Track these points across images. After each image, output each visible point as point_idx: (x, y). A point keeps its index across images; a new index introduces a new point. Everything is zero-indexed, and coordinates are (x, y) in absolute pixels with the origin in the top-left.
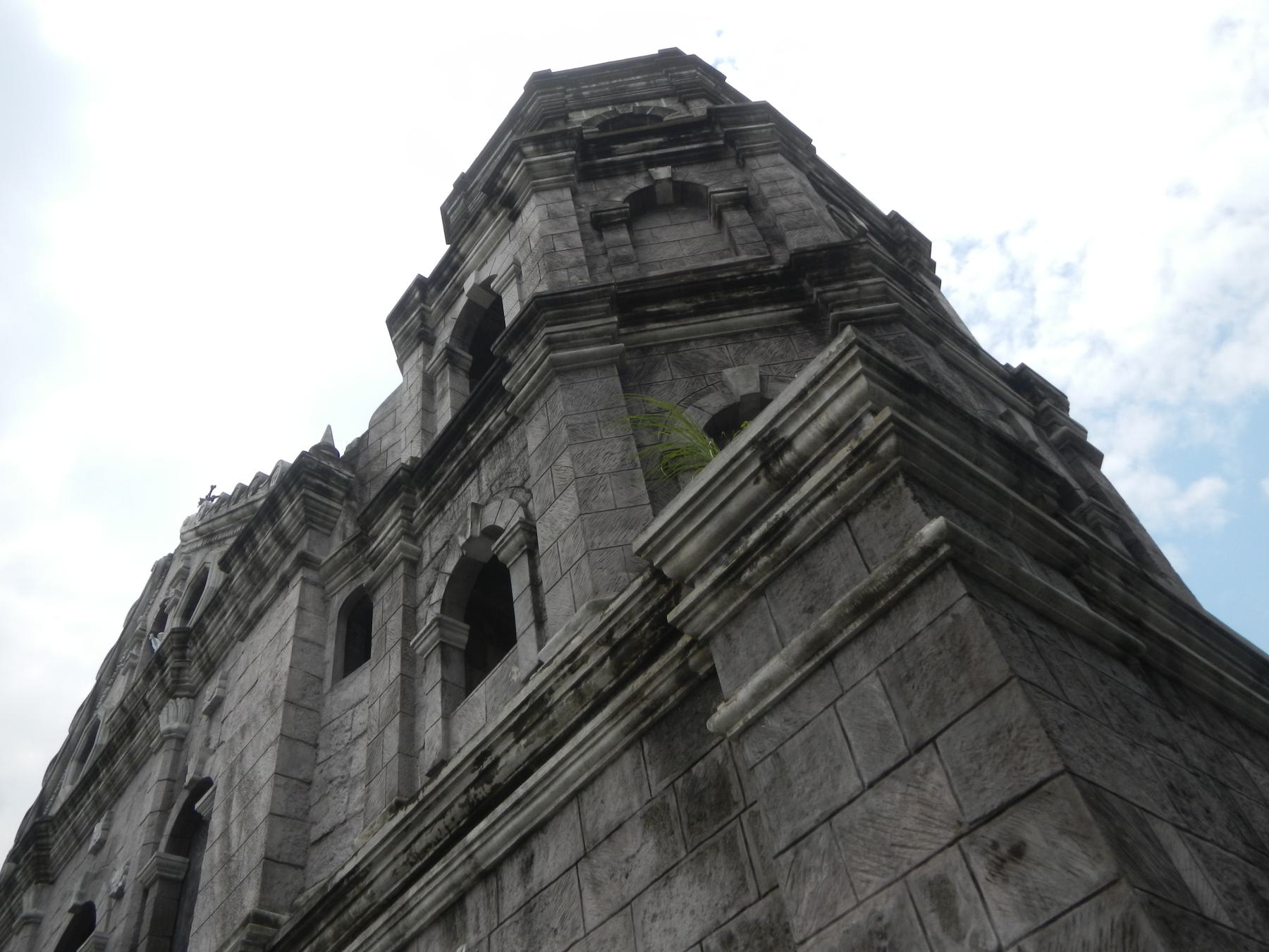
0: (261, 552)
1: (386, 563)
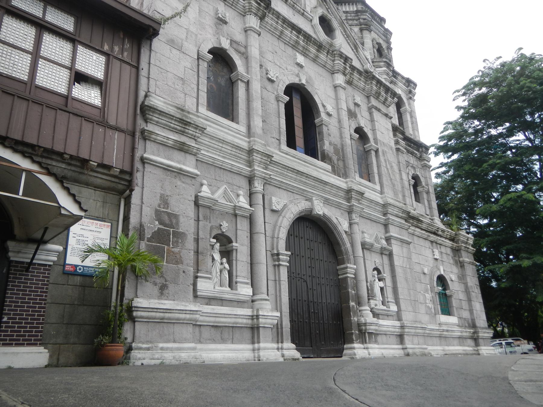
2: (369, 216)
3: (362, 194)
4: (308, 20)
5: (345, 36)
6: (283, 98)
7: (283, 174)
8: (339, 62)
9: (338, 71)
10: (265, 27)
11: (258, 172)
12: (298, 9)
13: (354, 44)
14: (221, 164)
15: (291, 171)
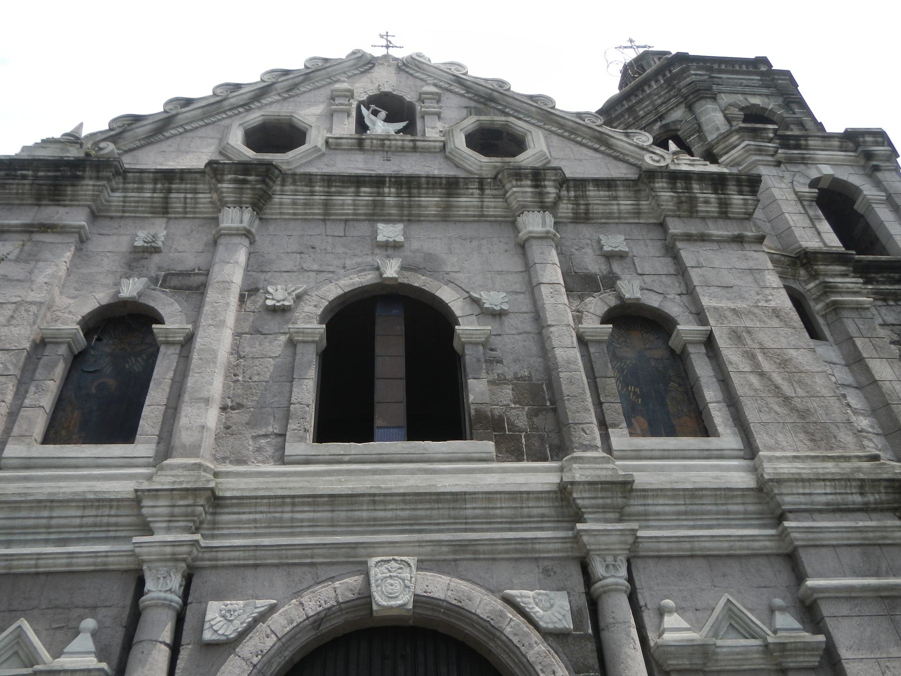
0: (701, 199)
1: (857, 301)
2: (687, 546)
3: (625, 486)
4: (435, 152)
5: (566, 134)
6: (303, 332)
7: (281, 520)
8: (515, 189)
9: (523, 208)
10: (281, 213)
11: (145, 550)
12: (397, 147)
13: (595, 138)
14: (33, 562)
15: (309, 504)
